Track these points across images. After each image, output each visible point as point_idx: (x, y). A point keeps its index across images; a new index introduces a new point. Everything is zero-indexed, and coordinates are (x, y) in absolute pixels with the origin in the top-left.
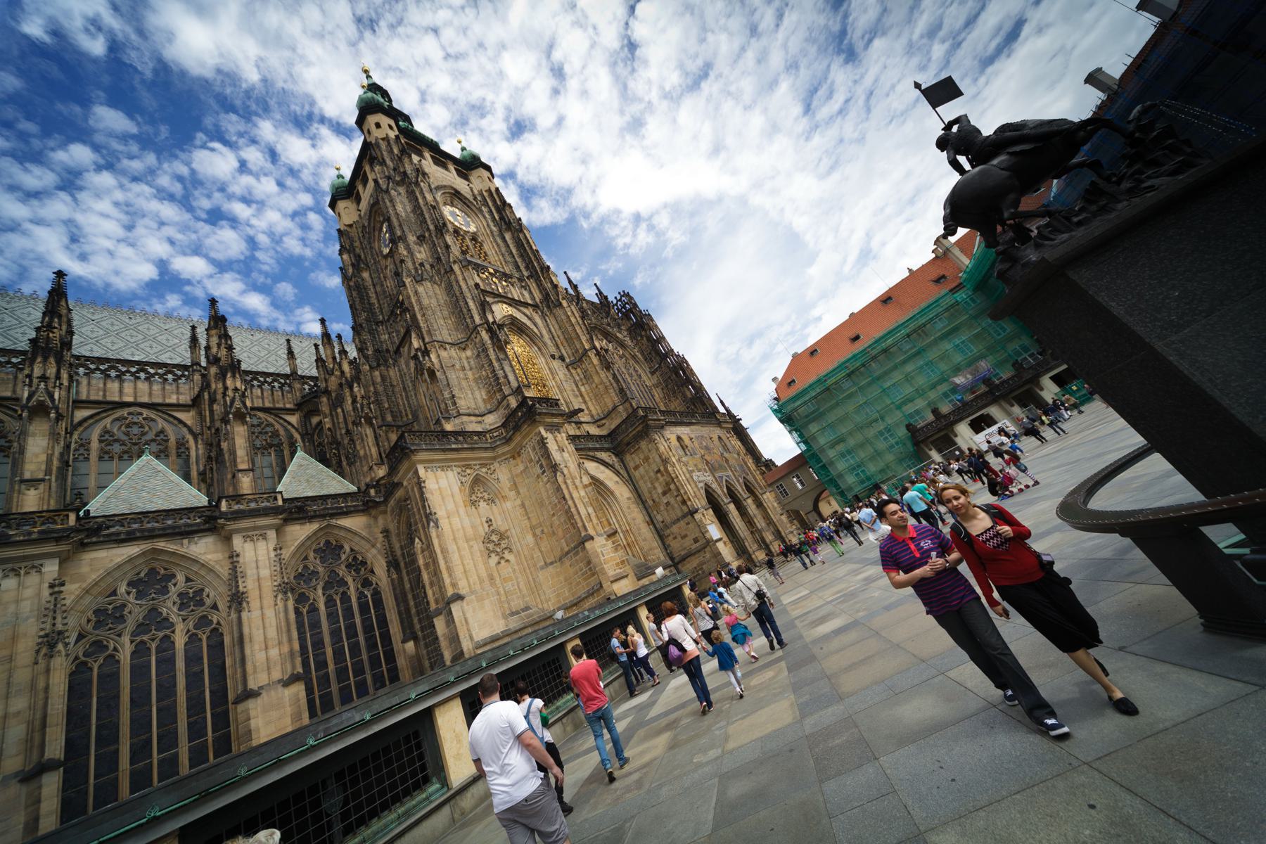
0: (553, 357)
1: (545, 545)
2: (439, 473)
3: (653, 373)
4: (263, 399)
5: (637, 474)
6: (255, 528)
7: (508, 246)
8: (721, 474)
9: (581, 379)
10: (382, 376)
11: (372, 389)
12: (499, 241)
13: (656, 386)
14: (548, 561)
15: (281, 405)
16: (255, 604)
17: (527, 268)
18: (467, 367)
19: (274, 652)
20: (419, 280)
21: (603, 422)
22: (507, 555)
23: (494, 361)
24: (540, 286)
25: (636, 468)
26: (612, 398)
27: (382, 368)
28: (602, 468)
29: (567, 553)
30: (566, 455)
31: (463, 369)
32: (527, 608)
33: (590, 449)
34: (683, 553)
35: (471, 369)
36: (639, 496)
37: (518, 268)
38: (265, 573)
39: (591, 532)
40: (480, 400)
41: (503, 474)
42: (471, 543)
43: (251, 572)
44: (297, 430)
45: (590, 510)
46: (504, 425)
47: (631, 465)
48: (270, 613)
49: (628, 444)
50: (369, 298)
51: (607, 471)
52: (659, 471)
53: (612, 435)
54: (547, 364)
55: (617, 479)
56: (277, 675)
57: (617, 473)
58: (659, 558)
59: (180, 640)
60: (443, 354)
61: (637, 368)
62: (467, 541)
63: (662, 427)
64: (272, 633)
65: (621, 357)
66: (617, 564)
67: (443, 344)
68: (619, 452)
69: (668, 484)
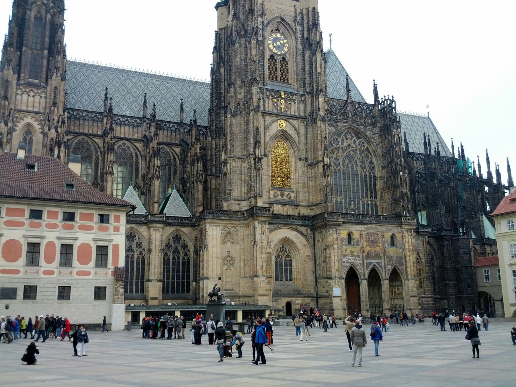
0: (300, 159)
1: (247, 269)
2: (214, 227)
3: (383, 168)
4: (167, 138)
5: (318, 244)
6: (156, 227)
7: (304, 64)
8: (371, 261)
9: (312, 177)
10: (216, 145)
11: (210, 152)
12: (300, 59)
13: (382, 178)
14: (245, 276)
15: (173, 142)
16: (154, 253)
17: (310, 84)
18: (243, 173)
19: (156, 270)
20: (233, 116)
21: (313, 208)
22: (231, 267)
23: (252, 177)
24: (312, 102)
25: (318, 241)
26: (320, 198)
27: (217, 139)
28: (299, 235)
29: (251, 277)
30: (264, 236)
31: (241, 173)
32: (232, 290)
33: (294, 225)
34: (322, 294)
35: (244, 174)
36: (315, 256)
37: (304, 84)
38: (157, 243)
39: (260, 273)
40: (243, 192)
41: (242, 232)
42: (218, 260)
43: (154, 242)
44: (178, 157)
45: (264, 264)
46: (246, 211)
47: (317, 238)
48: (157, 257)
49: (318, 227)
50: (221, 88)
51: (302, 238)
52: (325, 249)
53: (314, 217)
54: (295, 163)
55: (305, 243)
56: (156, 278)
57: (308, 240)
58: (311, 290)
59: (136, 257)
60: (234, 164)
61: (374, 160)
62: (217, 258)
63: (339, 225)
64: (157, 264)
65: (361, 152)
66: (266, 290)
67: (235, 158)
68: (313, 228)
69: (326, 258)
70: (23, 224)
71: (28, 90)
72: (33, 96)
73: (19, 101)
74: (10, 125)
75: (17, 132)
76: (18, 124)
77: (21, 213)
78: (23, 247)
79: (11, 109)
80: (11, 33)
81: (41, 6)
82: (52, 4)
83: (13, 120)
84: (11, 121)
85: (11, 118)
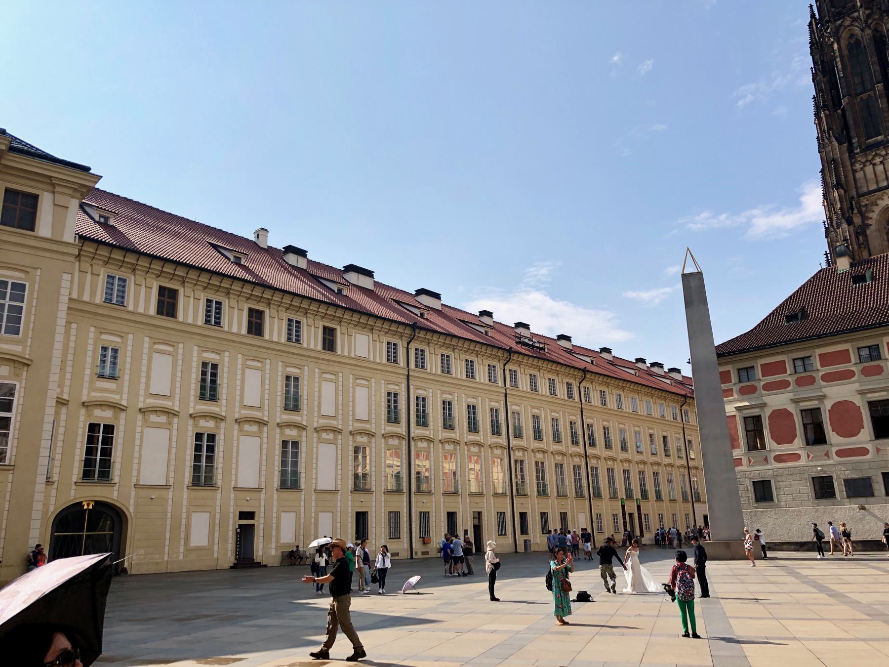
70: (851, 374)
71: (870, 157)
72: (882, 162)
73: (863, 181)
74: (857, 220)
75: (873, 228)
76: (871, 215)
77: (844, 357)
78: (862, 410)
79: (853, 198)
80: (818, 88)
81: (852, 25)
82: (867, 12)
83: (860, 212)
84: (858, 215)
85: (855, 211)
